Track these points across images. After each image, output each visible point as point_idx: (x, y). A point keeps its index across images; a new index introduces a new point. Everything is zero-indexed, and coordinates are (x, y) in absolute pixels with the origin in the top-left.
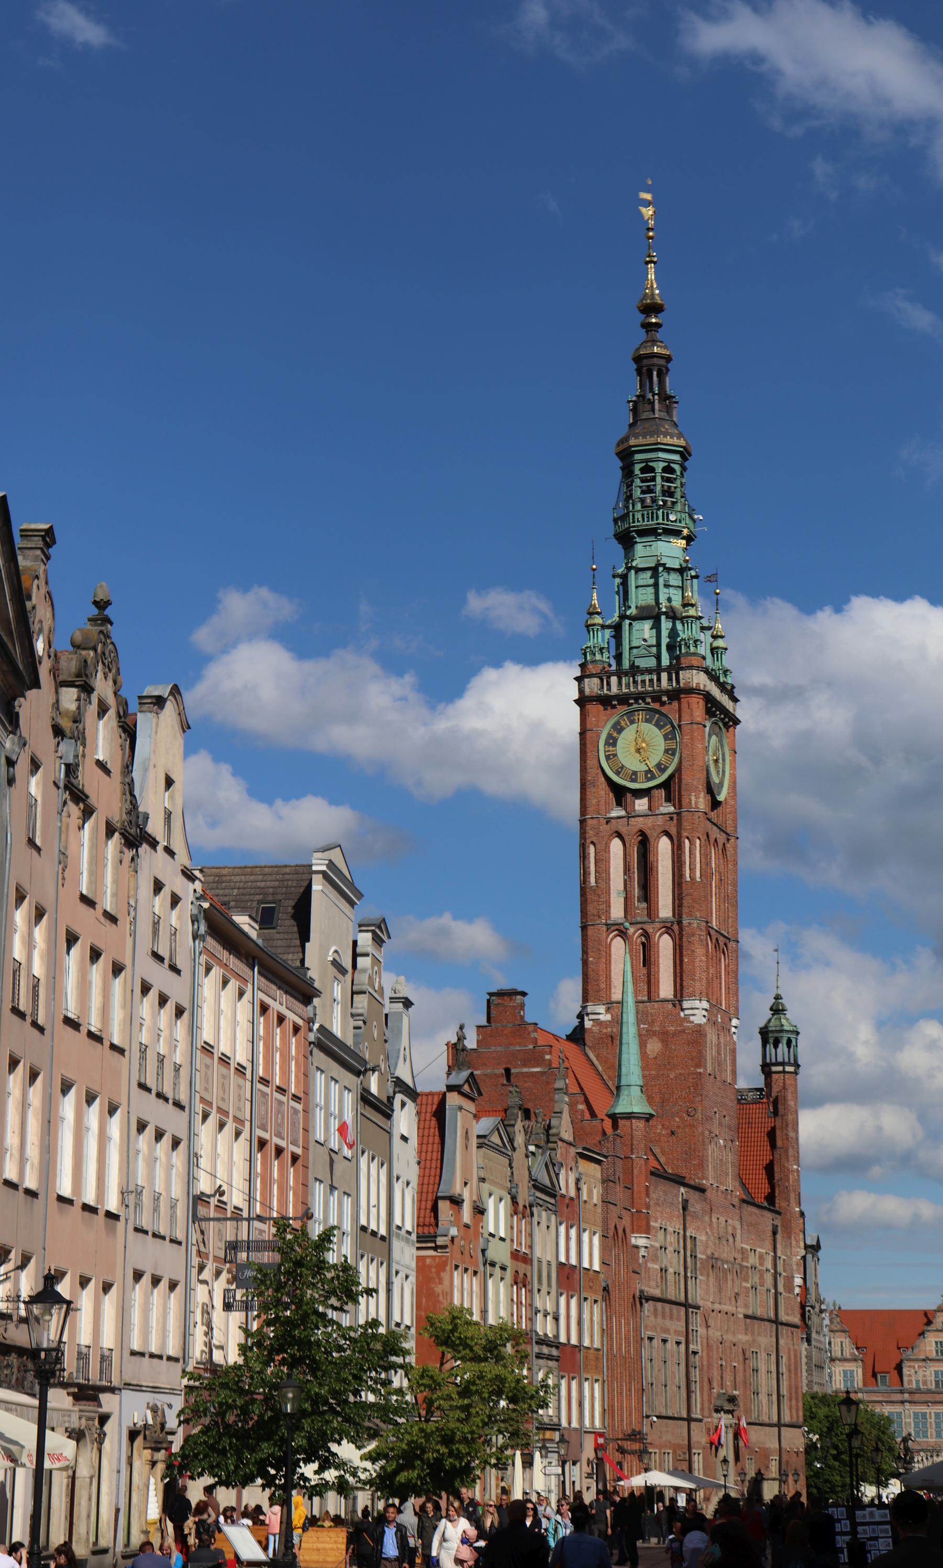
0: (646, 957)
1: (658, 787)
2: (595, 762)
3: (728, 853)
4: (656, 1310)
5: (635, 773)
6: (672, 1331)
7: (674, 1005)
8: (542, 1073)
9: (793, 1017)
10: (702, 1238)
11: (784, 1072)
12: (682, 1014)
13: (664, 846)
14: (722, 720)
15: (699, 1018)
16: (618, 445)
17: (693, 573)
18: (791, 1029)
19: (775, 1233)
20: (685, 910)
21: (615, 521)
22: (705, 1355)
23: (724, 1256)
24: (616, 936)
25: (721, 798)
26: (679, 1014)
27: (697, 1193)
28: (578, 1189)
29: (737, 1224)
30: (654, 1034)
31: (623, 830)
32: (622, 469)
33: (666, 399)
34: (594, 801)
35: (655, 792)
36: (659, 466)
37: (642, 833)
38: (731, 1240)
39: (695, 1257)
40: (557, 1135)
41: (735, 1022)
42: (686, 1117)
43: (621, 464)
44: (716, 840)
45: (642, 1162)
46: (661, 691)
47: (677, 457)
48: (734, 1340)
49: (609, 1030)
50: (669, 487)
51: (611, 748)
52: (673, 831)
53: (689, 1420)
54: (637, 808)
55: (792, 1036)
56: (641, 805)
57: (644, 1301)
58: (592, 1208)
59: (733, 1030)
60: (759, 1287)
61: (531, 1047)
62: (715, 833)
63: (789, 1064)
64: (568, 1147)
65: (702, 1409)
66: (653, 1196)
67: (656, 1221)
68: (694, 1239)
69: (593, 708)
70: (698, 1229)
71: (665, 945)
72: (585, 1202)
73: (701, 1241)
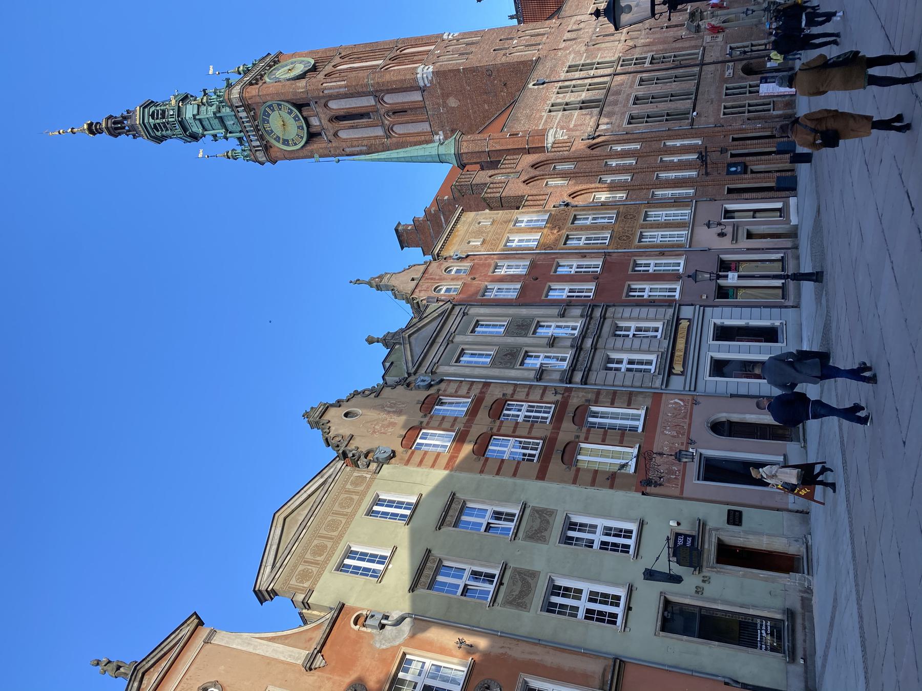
1: (300, 112)
5: (298, 127)
8: (444, 215)
10: (571, 60)
13: (333, 105)
14: (271, 67)
20: (365, 89)
27: (540, 67)
29: (574, 19)
30: (444, 102)
31: (332, 132)
35: (305, 114)
37: (331, 120)
38: (582, 25)
47: (146, 110)
52: (323, 101)
53: (702, 64)
56: (314, 121)
62: (329, 68)
65: (696, 47)
67: (541, 117)
68: (571, 68)
69: (273, 153)
70: (563, 63)
72: (484, 242)
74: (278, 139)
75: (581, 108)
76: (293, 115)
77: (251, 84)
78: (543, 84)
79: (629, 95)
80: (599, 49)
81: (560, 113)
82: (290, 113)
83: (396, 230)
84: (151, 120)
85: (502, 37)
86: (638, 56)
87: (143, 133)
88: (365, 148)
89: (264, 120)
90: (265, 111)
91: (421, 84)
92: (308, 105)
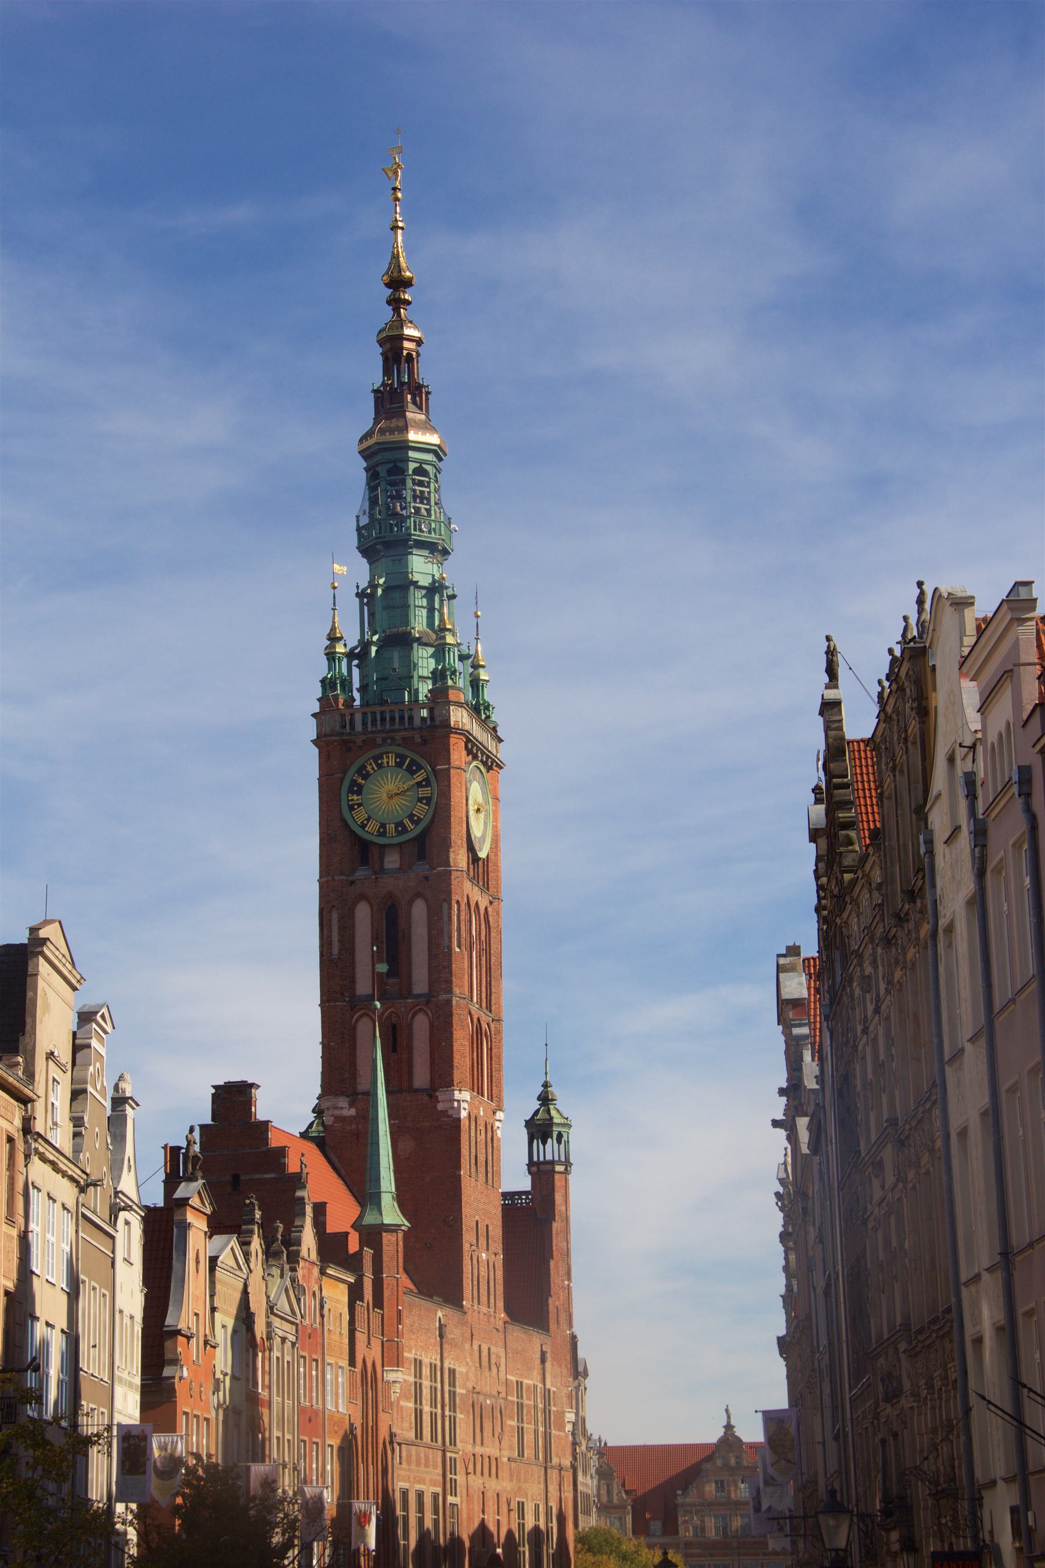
3: (491, 919)
4: (409, 1456)
6: (427, 1481)
7: (431, 1096)
10: (461, 1370)
11: (553, 1172)
12: (440, 1107)
14: (485, 764)
16: (361, 441)
17: (450, 592)
18: (562, 1121)
19: (543, 1360)
21: (359, 529)
22: (464, 1506)
23: (487, 1389)
24: (361, 1016)
25: (482, 854)
26: (435, 1107)
28: (322, 1316)
32: (367, 470)
33: (417, 389)
38: (494, 1369)
39: (454, 1392)
40: (298, 1252)
43: (365, 465)
44: (477, 903)
46: (414, 729)
47: (430, 457)
48: (498, 1488)
49: (354, 1126)
50: (422, 492)
51: (355, 797)
56: (392, 861)
57: (395, 1445)
59: (497, 1124)
60: (525, 1425)
61: (264, 1149)
62: (476, 895)
63: (560, 1162)
66: (407, 1320)
67: (410, 1352)
68: (452, 1372)
70: (457, 1358)
71: (421, 1025)
73: (461, 1373)
75: (416, 1409)
76: (407, 822)
77: (468, 741)
78: (441, 1336)
79: (421, 1481)
80: (468, 1412)
81: (412, 1379)
83: (252, 1085)
84: (412, 466)
85: (490, 1228)
86: (458, 1482)
87: (388, 438)
88: (335, 951)
89: (402, 758)
90: (420, 767)
92: (422, 856)
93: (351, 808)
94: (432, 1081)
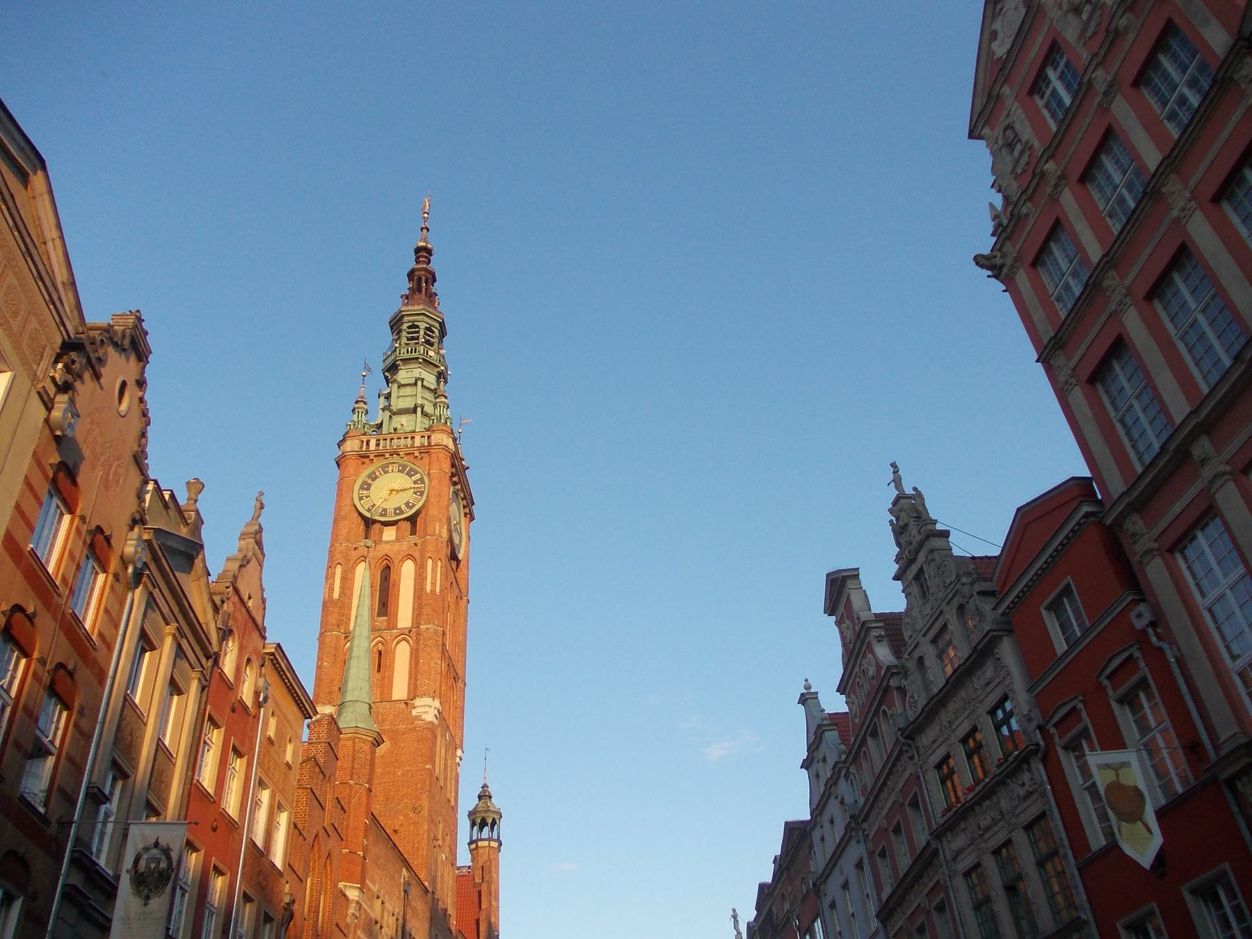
0: (381, 661)
1: (406, 519)
2: (349, 501)
9: (496, 802)
12: (414, 712)
13: (408, 569)
15: (430, 716)
34: (345, 531)
36: (423, 326)
41: (459, 752)
42: (412, 815)
45: (364, 793)
54: (385, 538)
55: (497, 817)
56: (389, 534)
58: (284, 768)
64: (250, 624)
67: (374, 883)
71: (402, 653)
74: (373, 477)
82: (407, 504)
88: (336, 595)
90: (416, 473)
91: (418, 702)
92: (413, 532)
93: (361, 499)
94: (409, 693)
